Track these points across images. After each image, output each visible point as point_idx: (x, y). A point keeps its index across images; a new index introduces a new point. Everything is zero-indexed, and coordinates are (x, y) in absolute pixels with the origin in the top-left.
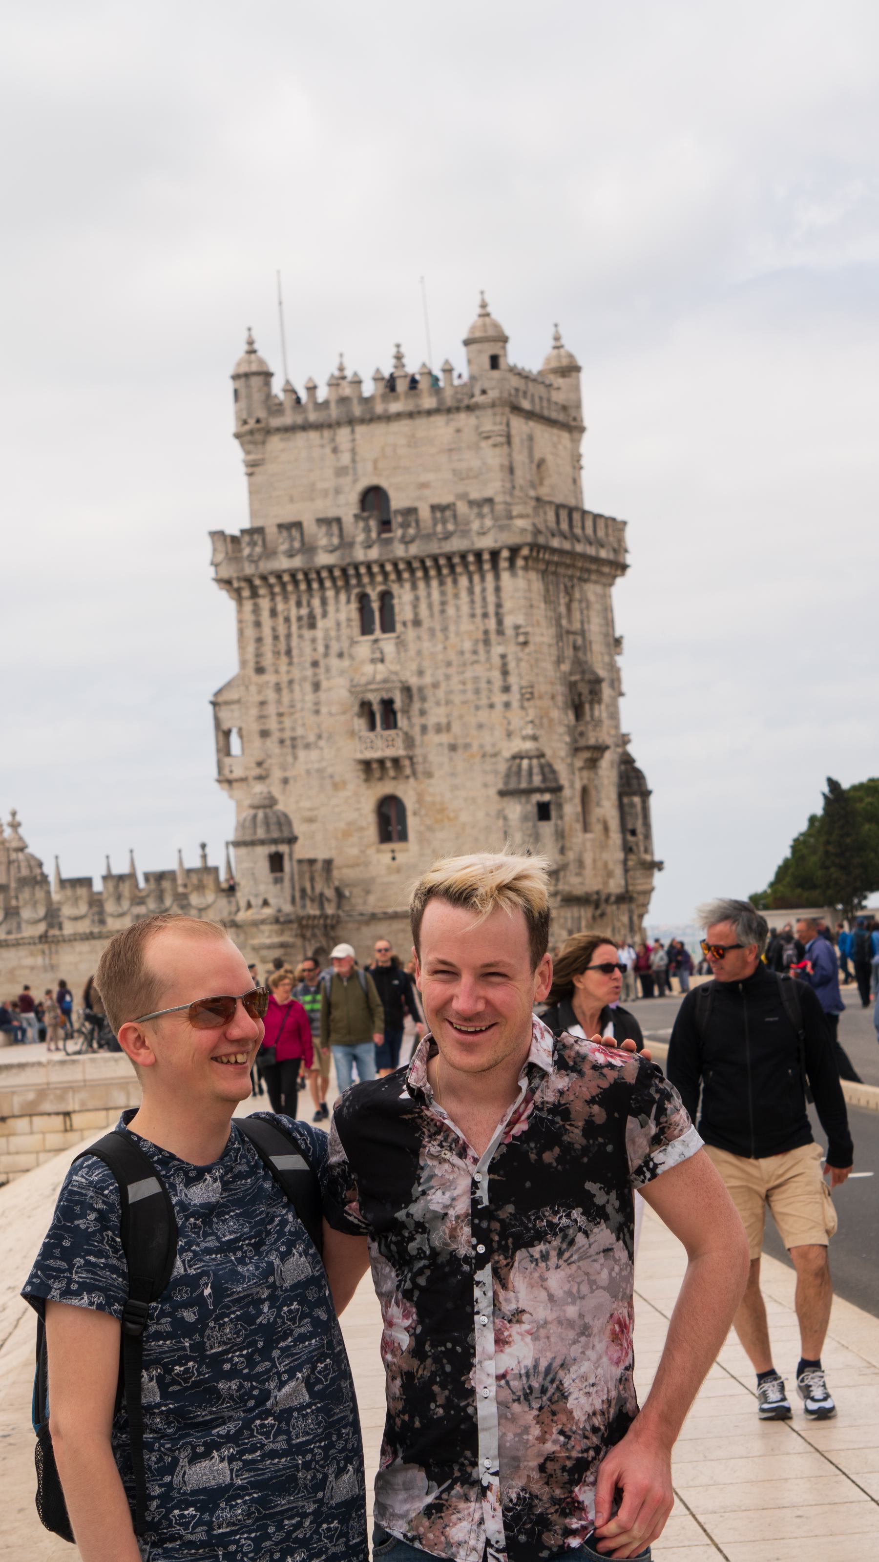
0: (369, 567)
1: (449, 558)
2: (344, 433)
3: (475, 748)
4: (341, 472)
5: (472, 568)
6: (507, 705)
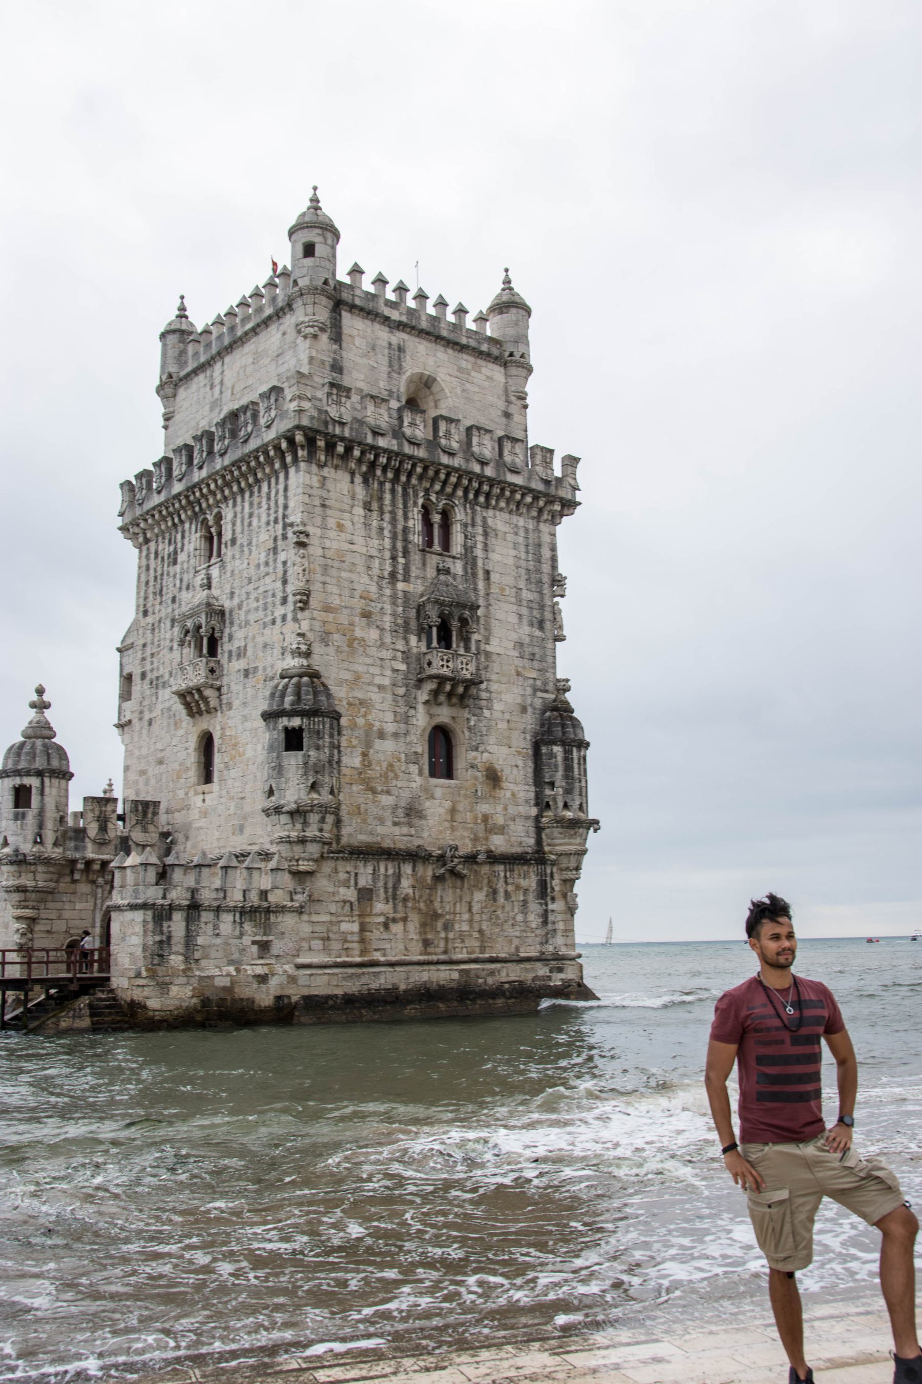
0: (201, 490)
1: (244, 459)
2: (218, 366)
3: (260, 672)
4: (215, 404)
5: (267, 470)
6: (284, 618)
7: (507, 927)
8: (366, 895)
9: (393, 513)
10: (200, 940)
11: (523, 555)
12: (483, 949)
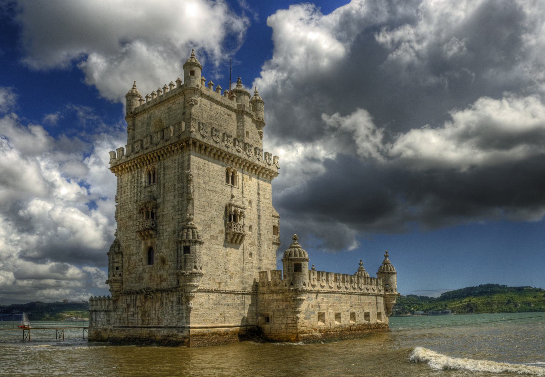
7: (166, 315)
8: (128, 306)
9: (137, 179)
10: (98, 319)
11: (177, 170)
12: (159, 323)
